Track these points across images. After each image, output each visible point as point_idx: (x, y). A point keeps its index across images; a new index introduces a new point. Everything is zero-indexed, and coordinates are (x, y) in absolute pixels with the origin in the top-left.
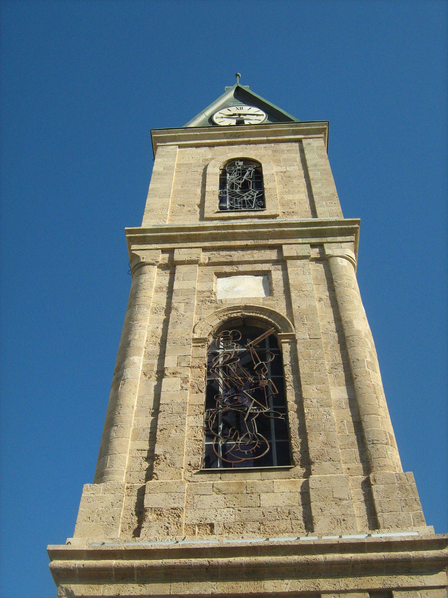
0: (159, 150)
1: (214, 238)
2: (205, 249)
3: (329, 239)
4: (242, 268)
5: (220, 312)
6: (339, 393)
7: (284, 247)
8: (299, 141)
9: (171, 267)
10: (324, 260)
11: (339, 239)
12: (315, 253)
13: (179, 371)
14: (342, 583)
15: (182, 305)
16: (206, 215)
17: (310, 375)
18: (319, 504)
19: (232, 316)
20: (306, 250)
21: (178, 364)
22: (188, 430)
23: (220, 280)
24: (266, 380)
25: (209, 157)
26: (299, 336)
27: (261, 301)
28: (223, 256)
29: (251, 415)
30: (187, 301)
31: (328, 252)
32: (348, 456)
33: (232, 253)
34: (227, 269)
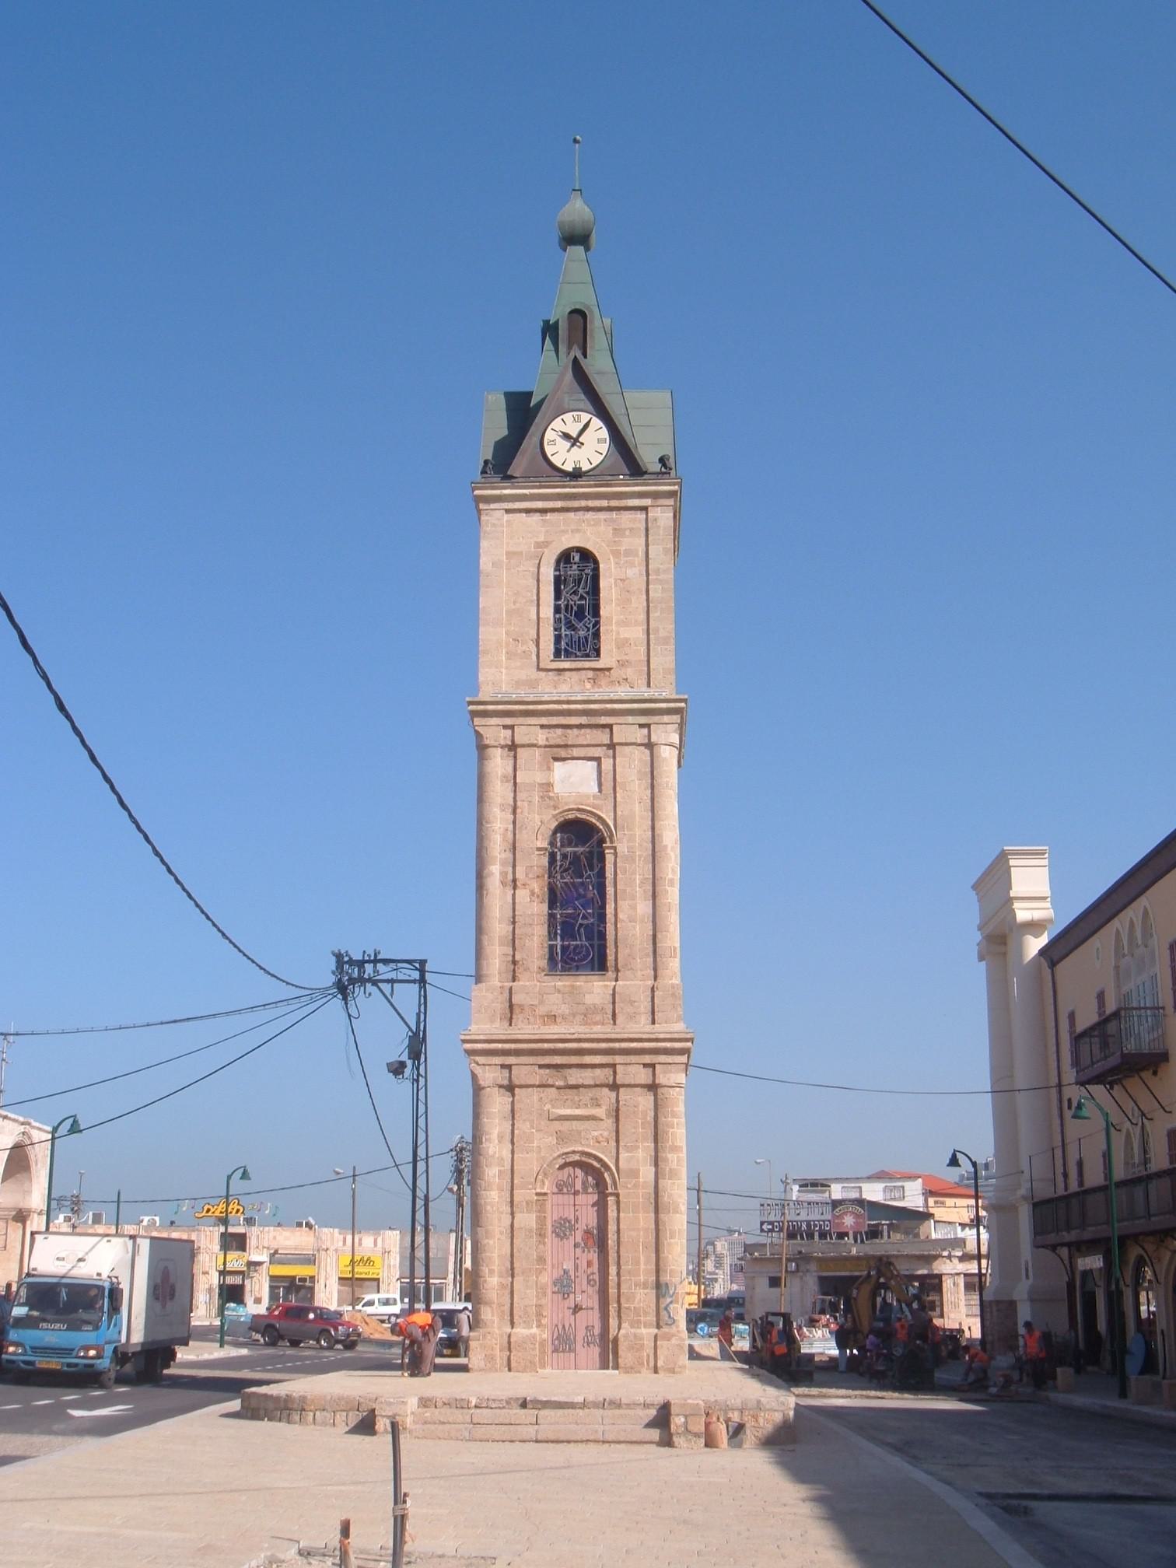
0: (483, 518)
2: (542, 726)
3: (656, 719)
6: (644, 908)
7: (615, 728)
8: (645, 509)
9: (513, 747)
10: (650, 746)
11: (666, 718)
12: (640, 735)
16: (542, 666)
22: (536, 940)
23: (557, 764)
24: (592, 892)
25: (542, 539)
32: (642, 962)
34: (563, 753)
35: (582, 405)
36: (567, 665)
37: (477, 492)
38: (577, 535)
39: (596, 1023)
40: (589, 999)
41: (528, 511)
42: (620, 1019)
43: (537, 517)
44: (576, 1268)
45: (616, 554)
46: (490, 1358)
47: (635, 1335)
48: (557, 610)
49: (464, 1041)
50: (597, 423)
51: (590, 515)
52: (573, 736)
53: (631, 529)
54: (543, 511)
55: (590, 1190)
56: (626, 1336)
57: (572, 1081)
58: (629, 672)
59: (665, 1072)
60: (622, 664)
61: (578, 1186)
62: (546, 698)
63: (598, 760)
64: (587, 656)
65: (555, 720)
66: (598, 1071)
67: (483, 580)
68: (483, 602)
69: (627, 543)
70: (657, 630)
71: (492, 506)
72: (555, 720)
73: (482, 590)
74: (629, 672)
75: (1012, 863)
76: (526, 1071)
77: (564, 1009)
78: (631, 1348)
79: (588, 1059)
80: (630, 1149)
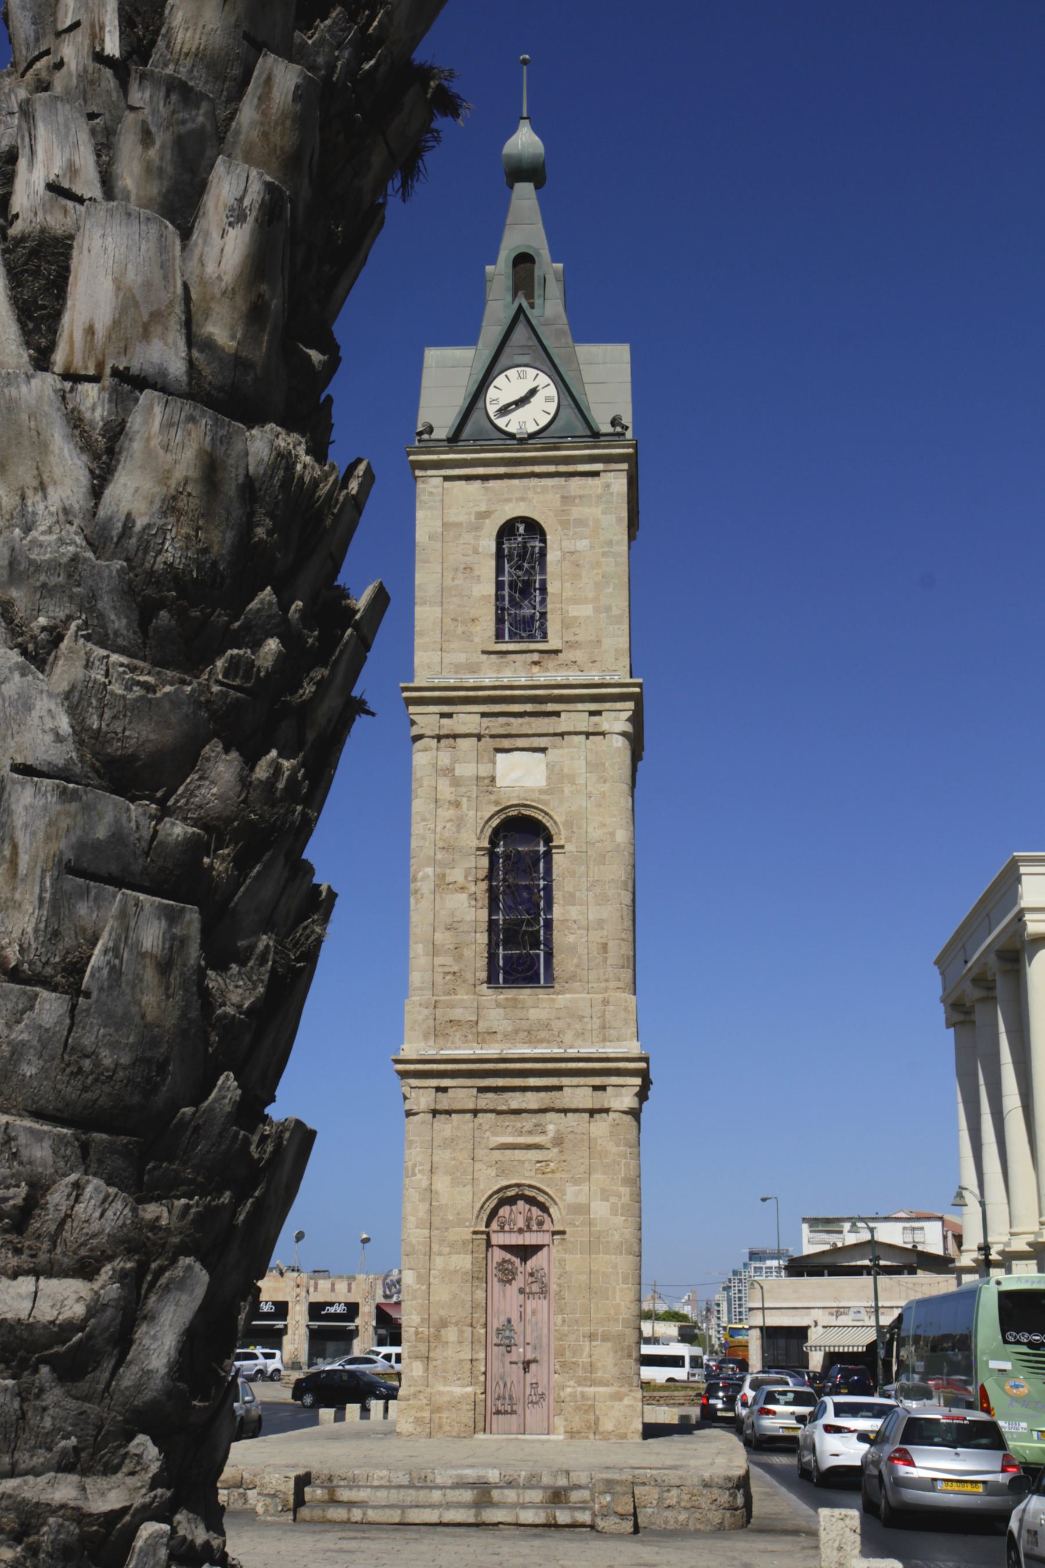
2: (484, 715)
5: (498, 812)
8: (595, 474)
11: (619, 705)
13: (467, 885)
14: (575, 1081)
15: (465, 800)
17: (572, 895)
18: (569, 1020)
19: (510, 814)
20: (583, 722)
21: (466, 877)
23: (500, 756)
25: (483, 508)
27: (537, 794)
28: (502, 726)
29: (525, 932)
30: (468, 794)
31: (605, 727)
33: (512, 720)
34: (506, 743)
35: (526, 359)
36: (511, 647)
37: (412, 458)
38: (522, 504)
39: (541, 1041)
40: (534, 1014)
42: (568, 1037)
43: (477, 484)
44: (522, 1316)
45: (565, 524)
46: (418, 1421)
47: (583, 1395)
48: (499, 585)
49: (398, 1061)
50: (543, 379)
51: (534, 481)
53: (581, 497)
55: (535, 1228)
56: (573, 1395)
57: (514, 1105)
58: (578, 655)
59: (617, 1096)
60: (571, 645)
61: (521, 1223)
62: (487, 682)
63: (543, 750)
64: (531, 638)
66: (543, 1094)
67: (419, 556)
68: (420, 578)
69: (577, 512)
70: (608, 609)
71: (430, 472)
73: (418, 565)
74: (578, 655)
75: (1022, 870)
76: (462, 1094)
77: (506, 1026)
78: (578, 1409)
79: (532, 1082)
80: (576, 1182)
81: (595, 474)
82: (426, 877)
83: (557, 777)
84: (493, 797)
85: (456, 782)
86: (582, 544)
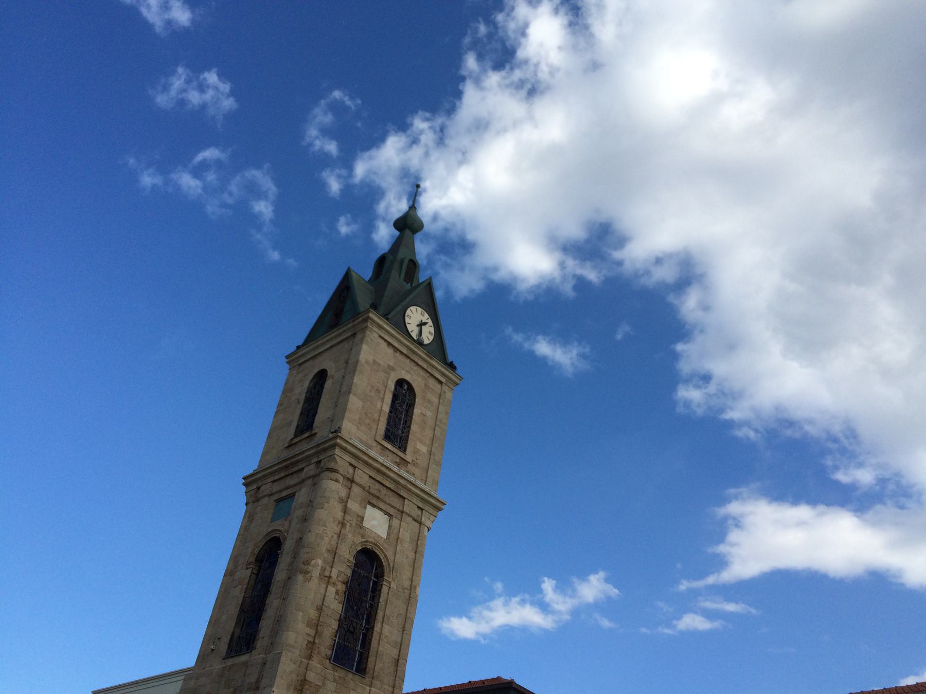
1: (379, 471)
3: (426, 508)
4: (381, 505)
8: (440, 382)
11: (431, 511)
17: (388, 618)
21: (338, 577)
23: (369, 507)
26: (393, 585)
31: (423, 520)
33: (381, 488)
34: (374, 501)
36: (389, 446)
41: (389, 344)
43: (390, 351)
45: (424, 398)
51: (416, 368)
52: (384, 491)
54: (396, 350)
58: (416, 471)
60: (415, 464)
65: (379, 478)
68: (356, 380)
71: (375, 329)
72: (379, 478)
73: (357, 373)
74: (416, 471)
81: (440, 382)
82: (316, 565)
83: (394, 536)
84: (362, 532)
85: (345, 510)
86: (429, 414)
